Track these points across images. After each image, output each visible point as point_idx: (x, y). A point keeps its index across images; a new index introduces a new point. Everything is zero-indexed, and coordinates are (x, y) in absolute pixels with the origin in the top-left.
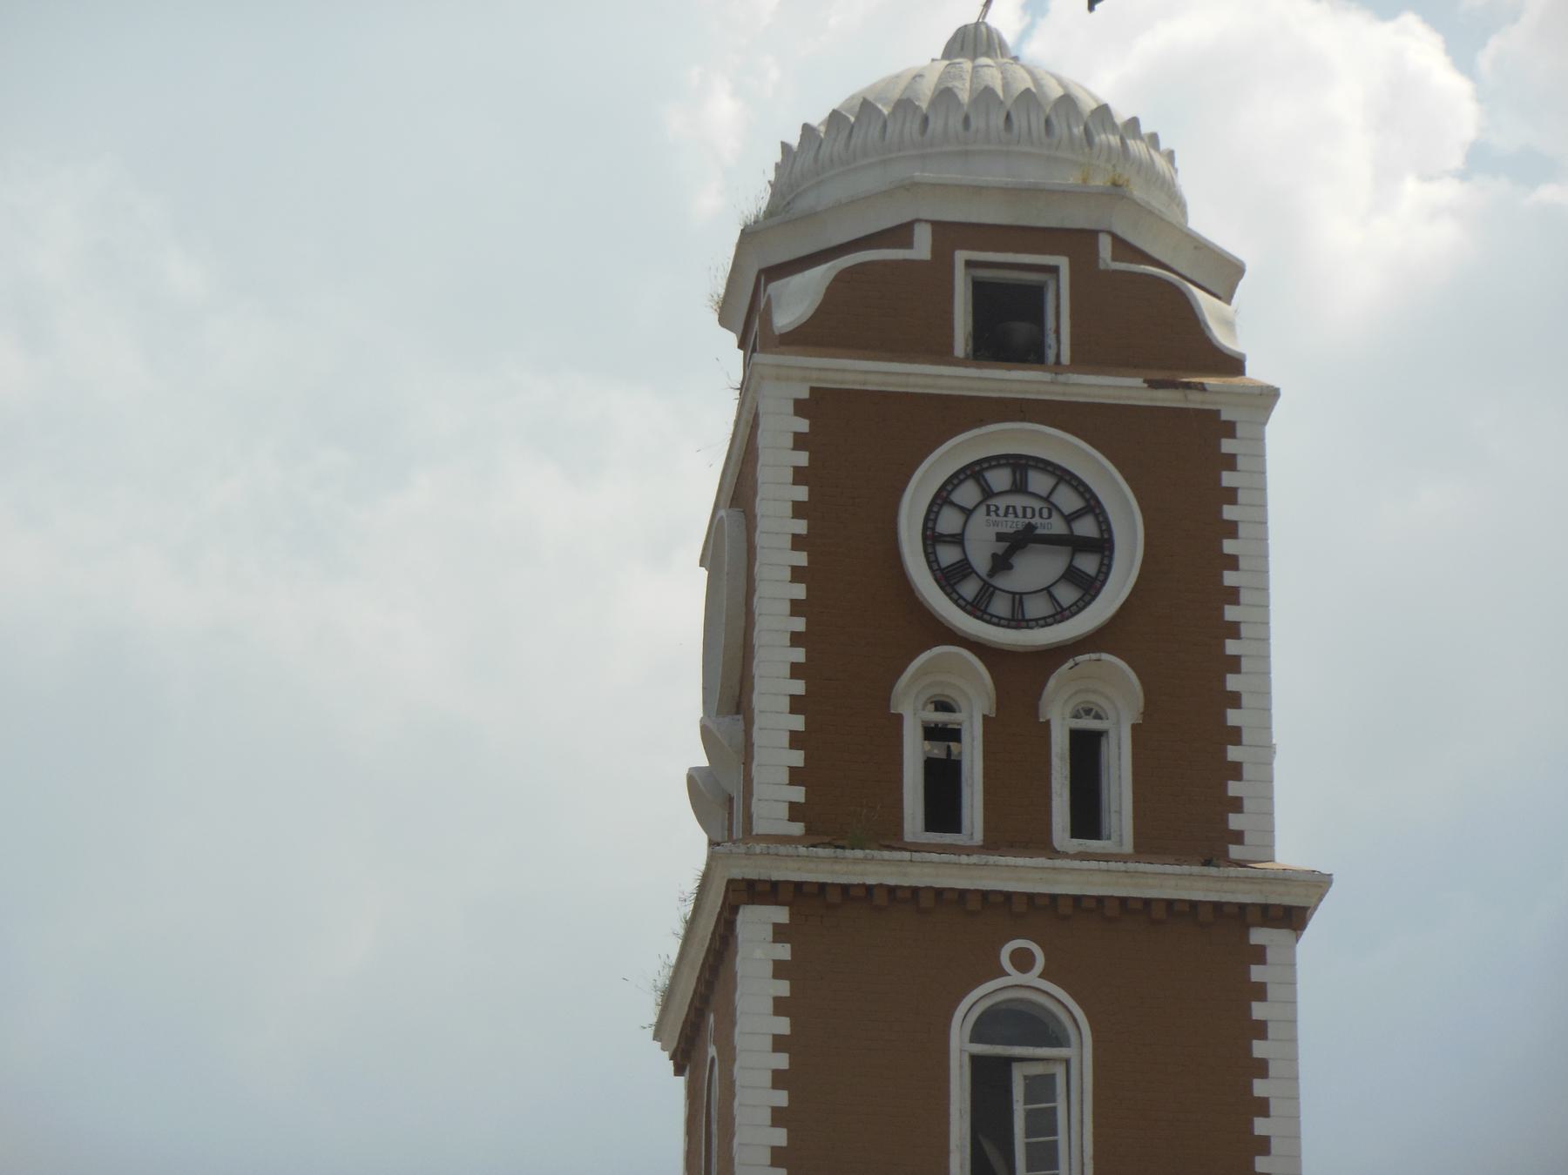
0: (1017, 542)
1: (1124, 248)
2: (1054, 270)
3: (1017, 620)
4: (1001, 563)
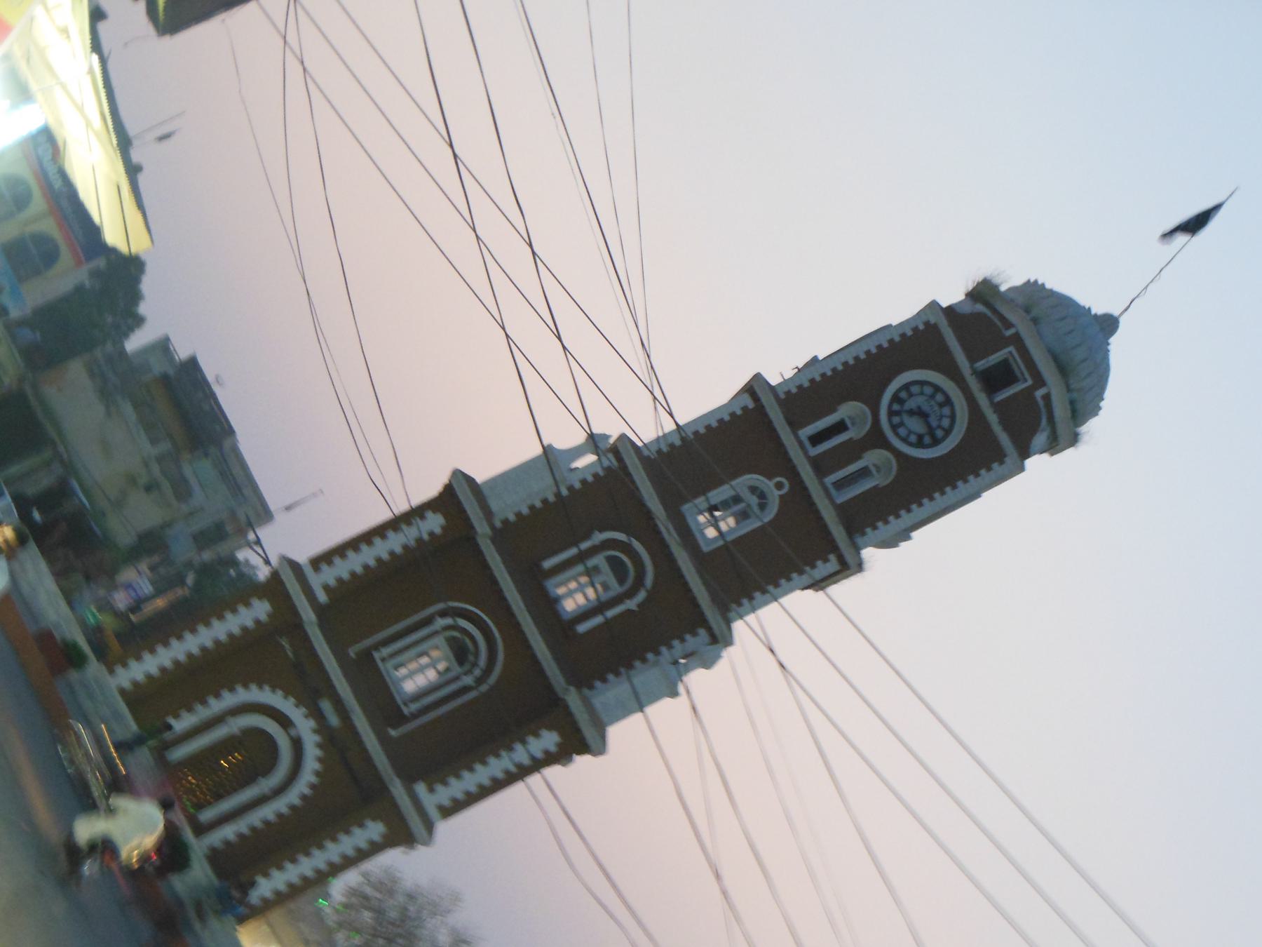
0: (921, 414)
1: (1047, 398)
2: (1026, 380)
3: (894, 428)
4: (911, 413)
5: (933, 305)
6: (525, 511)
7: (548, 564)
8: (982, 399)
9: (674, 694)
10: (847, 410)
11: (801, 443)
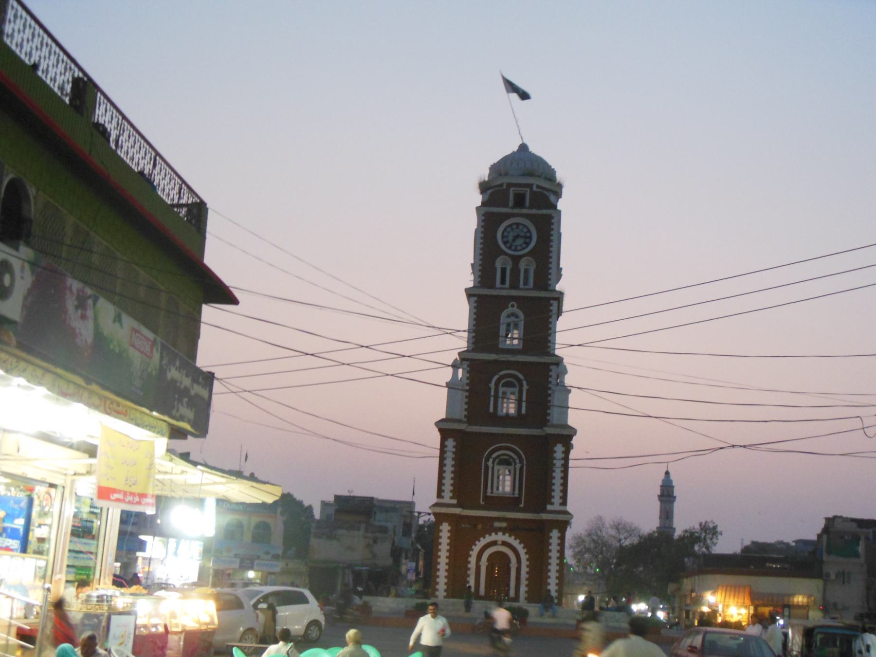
0: (517, 237)
1: (538, 187)
3: (516, 250)
4: (514, 240)
5: (477, 209)
6: (466, 407)
7: (491, 410)
8: (525, 211)
9: (570, 391)
10: (499, 264)
11: (501, 288)
